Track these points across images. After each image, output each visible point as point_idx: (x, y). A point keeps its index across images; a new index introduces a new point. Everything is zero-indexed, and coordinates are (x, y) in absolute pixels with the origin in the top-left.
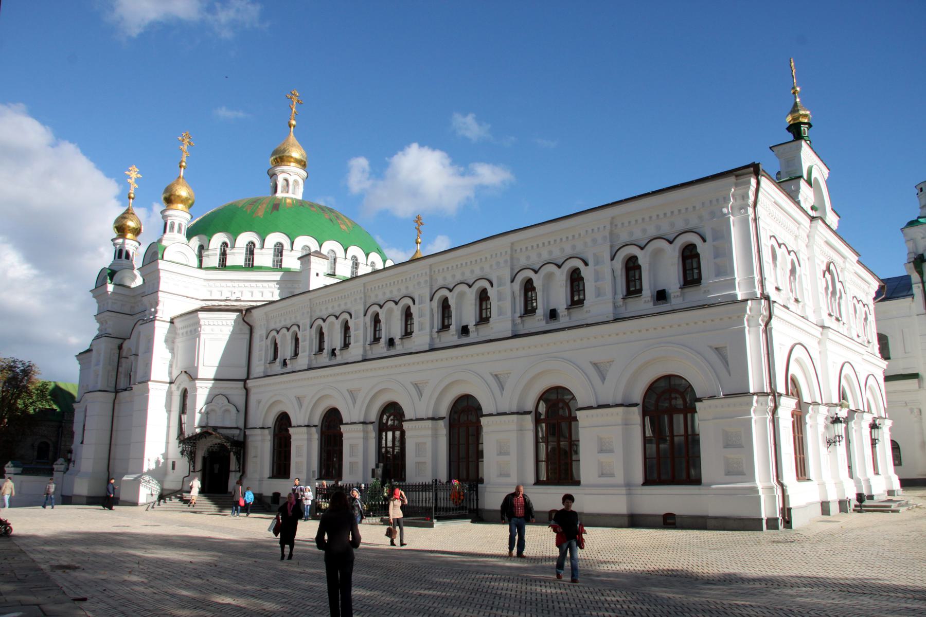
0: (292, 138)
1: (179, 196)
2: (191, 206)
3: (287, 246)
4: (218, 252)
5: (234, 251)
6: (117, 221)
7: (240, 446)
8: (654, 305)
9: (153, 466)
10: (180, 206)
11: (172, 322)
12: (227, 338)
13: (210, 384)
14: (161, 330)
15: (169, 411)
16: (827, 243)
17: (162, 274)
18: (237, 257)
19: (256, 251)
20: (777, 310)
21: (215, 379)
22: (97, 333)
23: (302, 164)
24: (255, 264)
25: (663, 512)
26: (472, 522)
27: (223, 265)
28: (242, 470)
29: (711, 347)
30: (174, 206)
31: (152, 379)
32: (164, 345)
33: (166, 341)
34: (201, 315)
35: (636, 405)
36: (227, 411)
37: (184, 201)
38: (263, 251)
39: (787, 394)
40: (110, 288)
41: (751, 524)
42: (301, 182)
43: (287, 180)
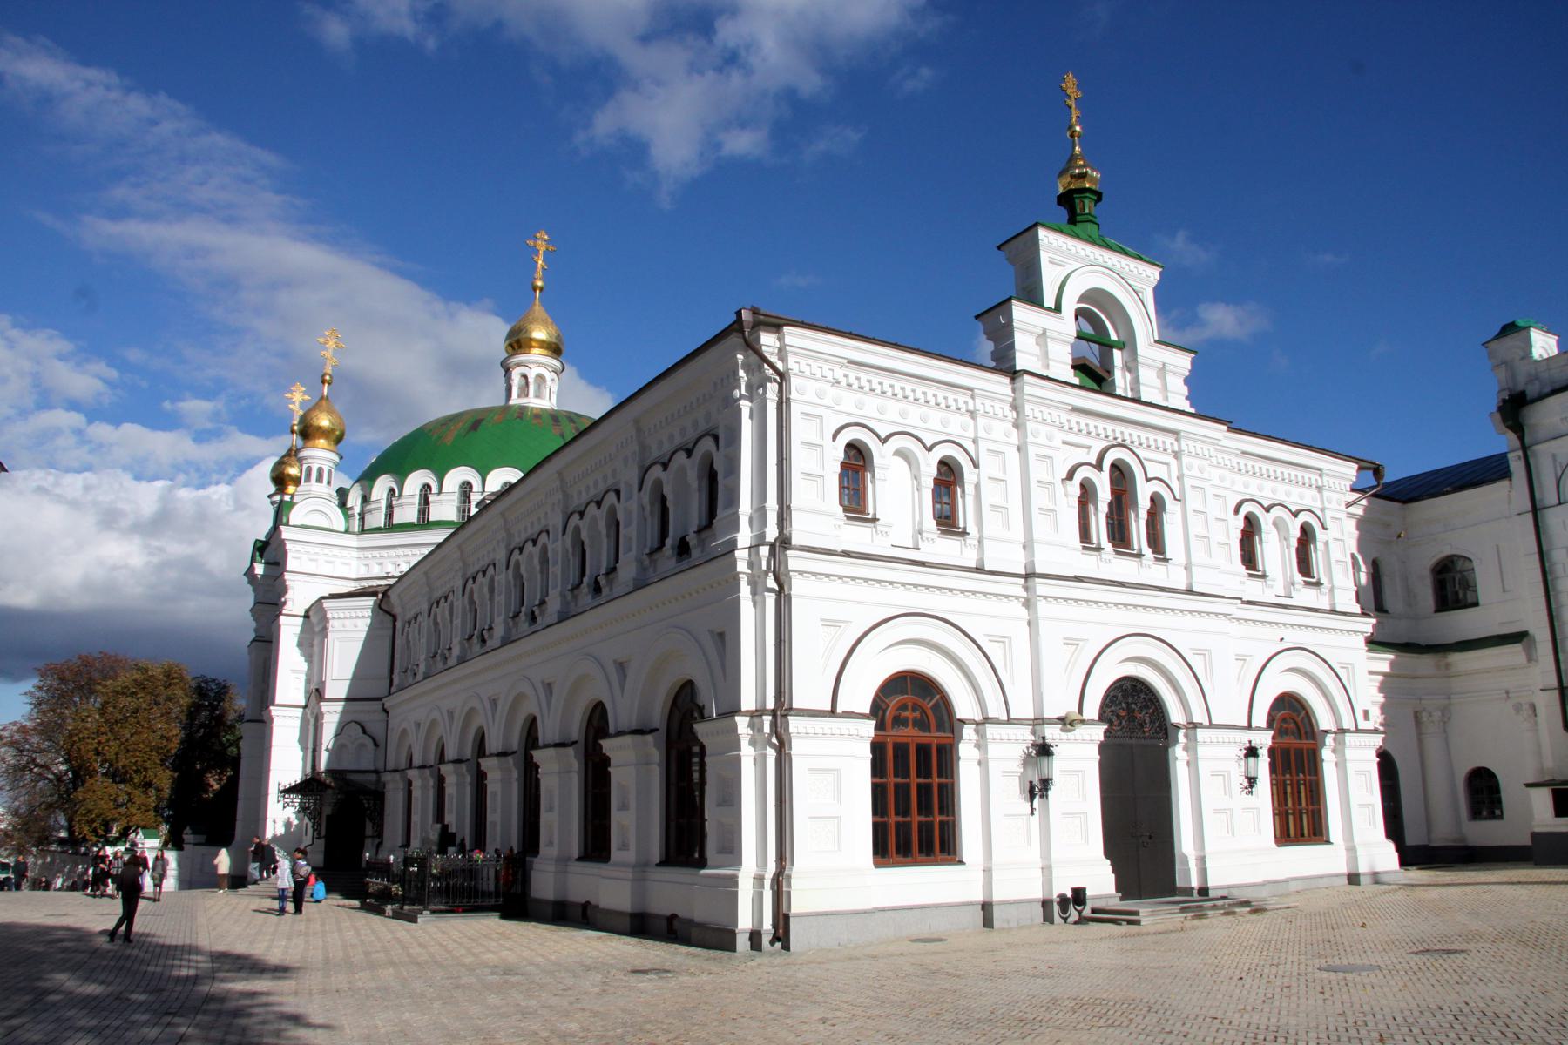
0: (537, 307)
1: (320, 428)
2: (339, 440)
3: (477, 487)
4: (383, 504)
5: (403, 500)
6: (274, 469)
7: (379, 796)
8: (678, 561)
9: (281, 830)
10: (322, 442)
11: (306, 616)
12: (363, 635)
13: (339, 707)
14: (289, 630)
15: (304, 749)
16: (1076, 410)
17: (289, 546)
18: (407, 512)
19: (431, 498)
20: (795, 560)
21: (347, 700)
22: (253, 636)
23: (555, 350)
24: (432, 519)
25: (668, 913)
26: (505, 916)
27: (390, 527)
28: (379, 834)
29: (711, 632)
30: (311, 443)
31: (278, 701)
32: (297, 651)
33: (300, 645)
34: (327, 604)
35: (652, 731)
36: (363, 745)
37: (326, 433)
38: (442, 497)
39: (833, 713)
40: (259, 569)
41: (719, 938)
42: (549, 375)
43: (525, 377)
